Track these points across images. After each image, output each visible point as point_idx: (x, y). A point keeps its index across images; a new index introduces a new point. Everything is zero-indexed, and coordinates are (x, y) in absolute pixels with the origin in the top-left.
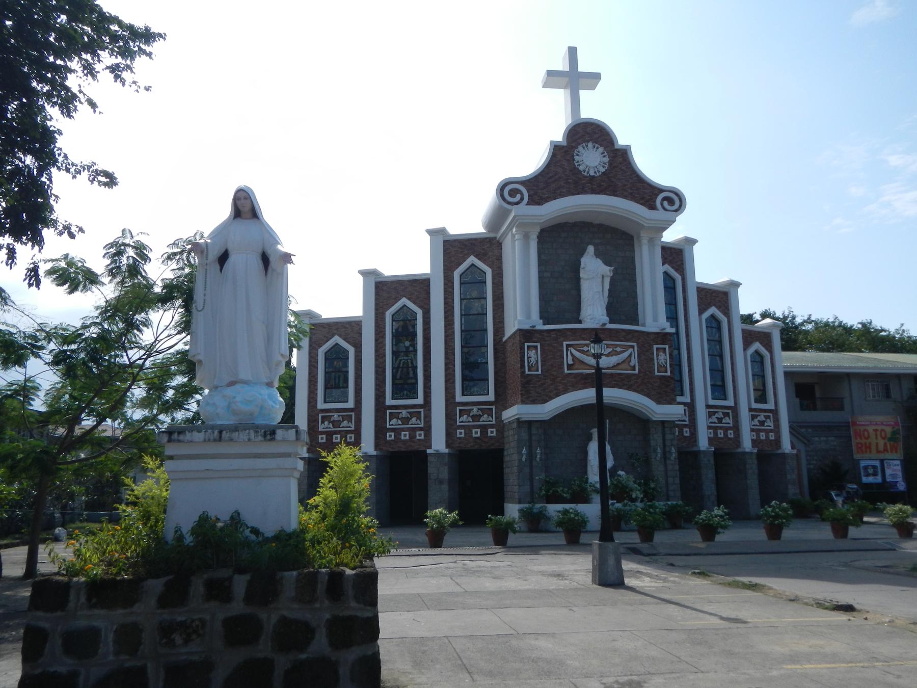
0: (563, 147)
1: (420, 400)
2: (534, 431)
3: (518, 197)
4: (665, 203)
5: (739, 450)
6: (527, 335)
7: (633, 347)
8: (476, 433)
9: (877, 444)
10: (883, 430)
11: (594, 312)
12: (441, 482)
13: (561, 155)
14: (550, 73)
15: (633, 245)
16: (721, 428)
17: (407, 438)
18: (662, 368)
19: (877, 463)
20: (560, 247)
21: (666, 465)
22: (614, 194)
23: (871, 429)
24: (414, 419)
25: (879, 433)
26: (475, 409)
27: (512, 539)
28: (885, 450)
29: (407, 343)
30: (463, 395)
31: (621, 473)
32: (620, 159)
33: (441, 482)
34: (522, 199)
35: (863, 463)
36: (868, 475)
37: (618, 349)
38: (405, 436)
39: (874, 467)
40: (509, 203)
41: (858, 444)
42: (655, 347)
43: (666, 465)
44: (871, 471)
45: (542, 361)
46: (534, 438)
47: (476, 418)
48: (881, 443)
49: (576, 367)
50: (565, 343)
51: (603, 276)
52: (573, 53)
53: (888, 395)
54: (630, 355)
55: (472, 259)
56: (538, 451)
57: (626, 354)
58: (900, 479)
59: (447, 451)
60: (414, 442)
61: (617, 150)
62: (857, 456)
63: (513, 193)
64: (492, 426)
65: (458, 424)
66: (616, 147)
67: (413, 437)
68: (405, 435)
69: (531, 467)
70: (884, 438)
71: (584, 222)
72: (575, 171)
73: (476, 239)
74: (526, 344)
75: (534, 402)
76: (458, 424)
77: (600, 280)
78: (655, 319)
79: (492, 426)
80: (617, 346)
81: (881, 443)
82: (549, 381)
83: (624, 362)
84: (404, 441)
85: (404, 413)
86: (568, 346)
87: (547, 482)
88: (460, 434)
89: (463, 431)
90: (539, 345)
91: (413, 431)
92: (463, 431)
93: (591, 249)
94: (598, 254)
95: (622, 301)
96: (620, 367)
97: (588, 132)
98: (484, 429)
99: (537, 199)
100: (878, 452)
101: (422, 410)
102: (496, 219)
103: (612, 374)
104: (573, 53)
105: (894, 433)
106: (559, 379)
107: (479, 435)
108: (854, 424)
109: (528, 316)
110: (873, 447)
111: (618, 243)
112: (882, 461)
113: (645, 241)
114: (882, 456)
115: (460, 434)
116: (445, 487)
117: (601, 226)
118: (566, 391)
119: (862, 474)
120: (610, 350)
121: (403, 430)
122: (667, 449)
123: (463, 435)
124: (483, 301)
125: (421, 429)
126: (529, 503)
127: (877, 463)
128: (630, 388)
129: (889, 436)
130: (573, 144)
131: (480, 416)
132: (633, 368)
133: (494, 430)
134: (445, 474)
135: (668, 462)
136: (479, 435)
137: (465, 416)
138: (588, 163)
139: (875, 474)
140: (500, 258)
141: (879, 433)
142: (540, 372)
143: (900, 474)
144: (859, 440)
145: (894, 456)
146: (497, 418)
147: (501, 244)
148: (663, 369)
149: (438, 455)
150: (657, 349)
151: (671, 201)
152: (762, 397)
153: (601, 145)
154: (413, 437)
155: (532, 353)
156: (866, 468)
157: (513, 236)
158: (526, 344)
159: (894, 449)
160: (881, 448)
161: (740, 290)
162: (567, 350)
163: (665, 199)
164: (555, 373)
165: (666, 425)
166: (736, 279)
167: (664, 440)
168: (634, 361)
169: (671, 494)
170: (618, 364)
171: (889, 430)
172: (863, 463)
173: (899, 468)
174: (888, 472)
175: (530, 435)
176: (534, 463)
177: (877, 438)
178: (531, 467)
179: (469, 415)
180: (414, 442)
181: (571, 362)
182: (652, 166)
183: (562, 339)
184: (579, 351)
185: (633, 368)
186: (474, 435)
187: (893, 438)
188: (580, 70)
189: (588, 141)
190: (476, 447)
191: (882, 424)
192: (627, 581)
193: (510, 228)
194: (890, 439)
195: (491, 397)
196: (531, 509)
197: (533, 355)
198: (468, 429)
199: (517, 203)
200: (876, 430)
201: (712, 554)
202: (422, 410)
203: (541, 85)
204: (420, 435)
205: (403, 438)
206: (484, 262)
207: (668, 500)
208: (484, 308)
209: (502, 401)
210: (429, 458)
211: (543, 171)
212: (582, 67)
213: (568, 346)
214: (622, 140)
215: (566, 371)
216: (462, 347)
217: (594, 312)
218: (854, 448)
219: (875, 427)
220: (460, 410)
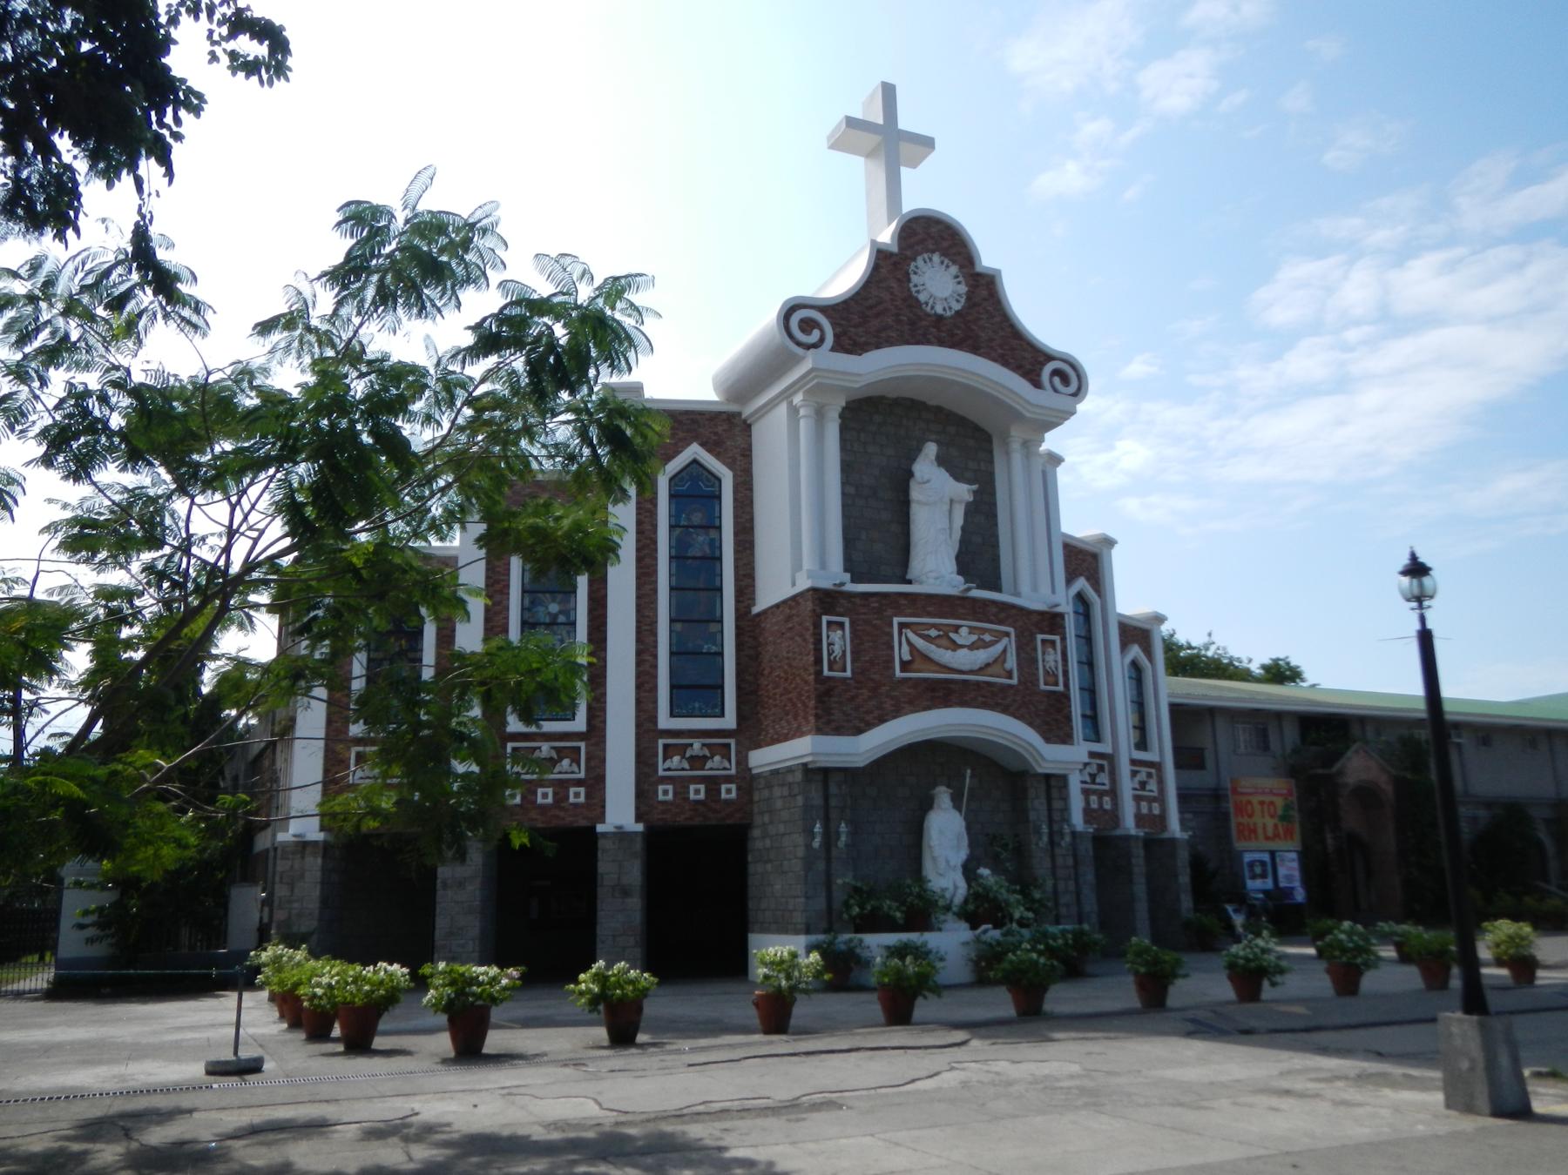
0: (891, 255)
1: (580, 723)
2: (833, 789)
3: (816, 335)
4: (1057, 380)
5: (1118, 832)
6: (825, 600)
7: (1007, 634)
8: (697, 792)
10: (1272, 803)
11: (935, 565)
12: (626, 893)
13: (888, 267)
14: (851, 122)
15: (991, 452)
16: (1094, 792)
17: (550, 800)
18: (1051, 676)
19: (1266, 857)
20: (880, 438)
21: (1053, 857)
22: (975, 350)
23: (1255, 800)
24: (566, 762)
26: (697, 744)
27: (802, 1010)
28: (1276, 836)
29: (554, 608)
30: (672, 715)
31: (984, 872)
32: (984, 289)
33: (626, 893)
34: (822, 340)
35: (1247, 857)
36: (1254, 877)
37: (987, 637)
38: (544, 796)
39: (1263, 863)
40: (799, 344)
41: (1239, 824)
42: (1040, 637)
43: (1053, 857)
44: (1258, 870)
45: (852, 652)
46: (833, 802)
47: (697, 762)
48: (1270, 822)
49: (915, 666)
50: (896, 620)
51: (952, 501)
52: (889, 92)
53: (1265, 747)
54: (1005, 651)
55: (694, 451)
56: (843, 827)
57: (999, 647)
58: (1297, 884)
59: (640, 827)
60: (562, 809)
61: (979, 275)
62: (1239, 845)
63: (808, 325)
64: (728, 779)
65: (661, 773)
66: (978, 269)
67: (561, 797)
68: (545, 796)
69: (828, 860)
70: (1272, 817)
71: (912, 400)
72: (912, 302)
73: (701, 413)
74: (825, 619)
75: (838, 731)
76: (661, 773)
77: (946, 507)
78: (1035, 588)
79: (728, 779)
80: (984, 631)
81: (1270, 822)
82: (865, 693)
83: (995, 661)
84: (543, 807)
85: (545, 749)
86: (902, 626)
87: (857, 890)
88: (665, 793)
89: (670, 788)
90: (846, 621)
91: (562, 786)
92: (670, 788)
93: (931, 449)
94: (942, 461)
95: (979, 551)
96: (990, 670)
97: (929, 236)
98: (713, 784)
99: (848, 344)
100: (1267, 838)
101: (582, 745)
102: (754, 376)
103: (978, 683)
104: (889, 92)
105: (1287, 807)
106: (884, 689)
107: (702, 796)
108: (1235, 791)
109: (823, 564)
110: (1260, 831)
111: (974, 443)
112: (1273, 854)
113: (1016, 446)
114: (1272, 845)
115: (665, 793)
116: (635, 903)
117: (939, 410)
118: (897, 712)
119: (1247, 873)
120: (974, 638)
121: (541, 783)
122: (1056, 827)
123: (670, 796)
124: (713, 534)
125: (579, 783)
126: (826, 932)
128: (1005, 710)
129: (1280, 812)
130: (908, 253)
131: (705, 759)
132: (1009, 675)
133: (733, 787)
134: (634, 874)
135: (1058, 851)
136: (702, 796)
137: (676, 759)
138: (933, 290)
139: (1264, 876)
140: (747, 453)
142: (849, 674)
143: (1297, 874)
144: (1240, 820)
145: (1289, 845)
146: (738, 763)
147: (749, 426)
148: (1051, 679)
149: (621, 835)
150: (1043, 641)
151: (1065, 380)
152: (1142, 745)
153: (954, 262)
154: (561, 797)
155: (836, 636)
156: (1251, 864)
157: (794, 411)
158: (825, 619)
159: (1289, 834)
160: (1270, 832)
161: (1116, 553)
162: (900, 634)
163: (1056, 372)
164: (876, 677)
165: (1053, 782)
166: (1112, 534)
167: (1050, 810)
168: (1011, 662)
169: (1063, 911)
170: (988, 665)
171: (1279, 802)
172: (1247, 857)
173: (1295, 865)
174: (1282, 871)
175: (826, 798)
176: (834, 852)
178: (828, 860)
179: (683, 757)
180: (562, 809)
181: (907, 657)
182: (1036, 311)
183: (889, 612)
184: (921, 636)
185: (1009, 675)
186: (692, 796)
187: (1285, 818)
188: (901, 126)
189: (933, 252)
190: (697, 821)
191: (1271, 793)
192: (1538, 1107)
193: (787, 394)
195: (729, 721)
196: (831, 943)
197: (838, 640)
198: (681, 784)
199: (815, 346)
200: (1262, 803)
201: (1292, 1031)
202: (582, 745)
203: (825, 145)
204: (577, 795)
205: (540, 800)
206: (718, 456)
207: (1058, 923)
208: (717, 545)
209: (752, 731)
210: (601, 843)
211: (857, 293)
212: (905, 123)
213: (902, 626)
214: (988, 258)
215: (898, 673)
216: (672, 621)
217: (935, 565)
218: (1234, 832)
219: (1261, 798)
220: (666, 747)
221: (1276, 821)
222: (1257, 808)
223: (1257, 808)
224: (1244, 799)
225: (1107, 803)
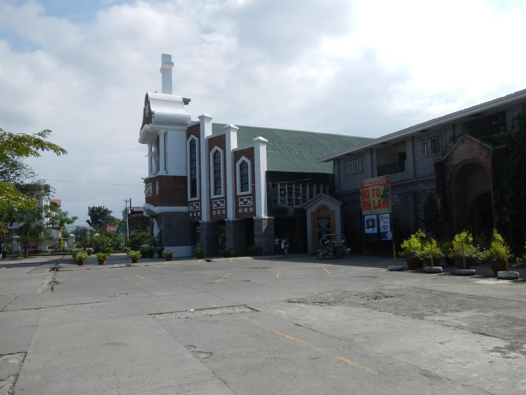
9: (374, 201)
16: (219, 209)
19: (375, 217)
23: (370, 189)
25: (375, 192)
28: (380, 206)
35: (366, 218)
36: (368, 228)
39: (373, 220)
41: (363, 202)
48: (376, 199)
70: (378, 196)
81: (376, 199)
100: (375, 208)
105: (385, 190)
108: (362, 187)
110: (372, 205)
112: (378, 215)
127: (375, 217)
129: (381, 194)
139: (373, 227)
141: (375, 192)
143: (389, 225)
144: (364, 200)
156: (368, 221)
159: (386, 204)
160: (376, 205)
171: (382, 188)
173: (388, 220)
174: (382, 224)
177: (374, 197)
191: (378, 184)
194: (382, 197)
200: (373, 190)
219: (373, 188)
221: (380, 198)
222: (371, 193)
223: (371, 193)
224: (366, 189)
225: (224, 212)
